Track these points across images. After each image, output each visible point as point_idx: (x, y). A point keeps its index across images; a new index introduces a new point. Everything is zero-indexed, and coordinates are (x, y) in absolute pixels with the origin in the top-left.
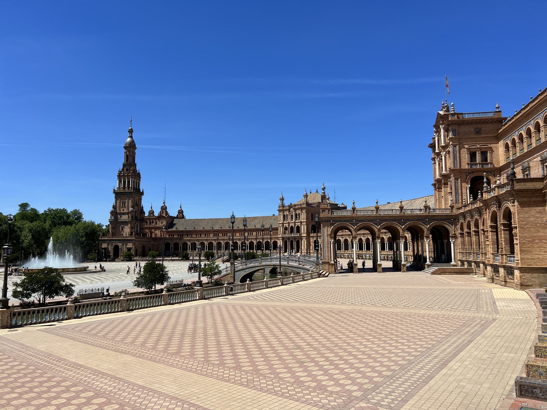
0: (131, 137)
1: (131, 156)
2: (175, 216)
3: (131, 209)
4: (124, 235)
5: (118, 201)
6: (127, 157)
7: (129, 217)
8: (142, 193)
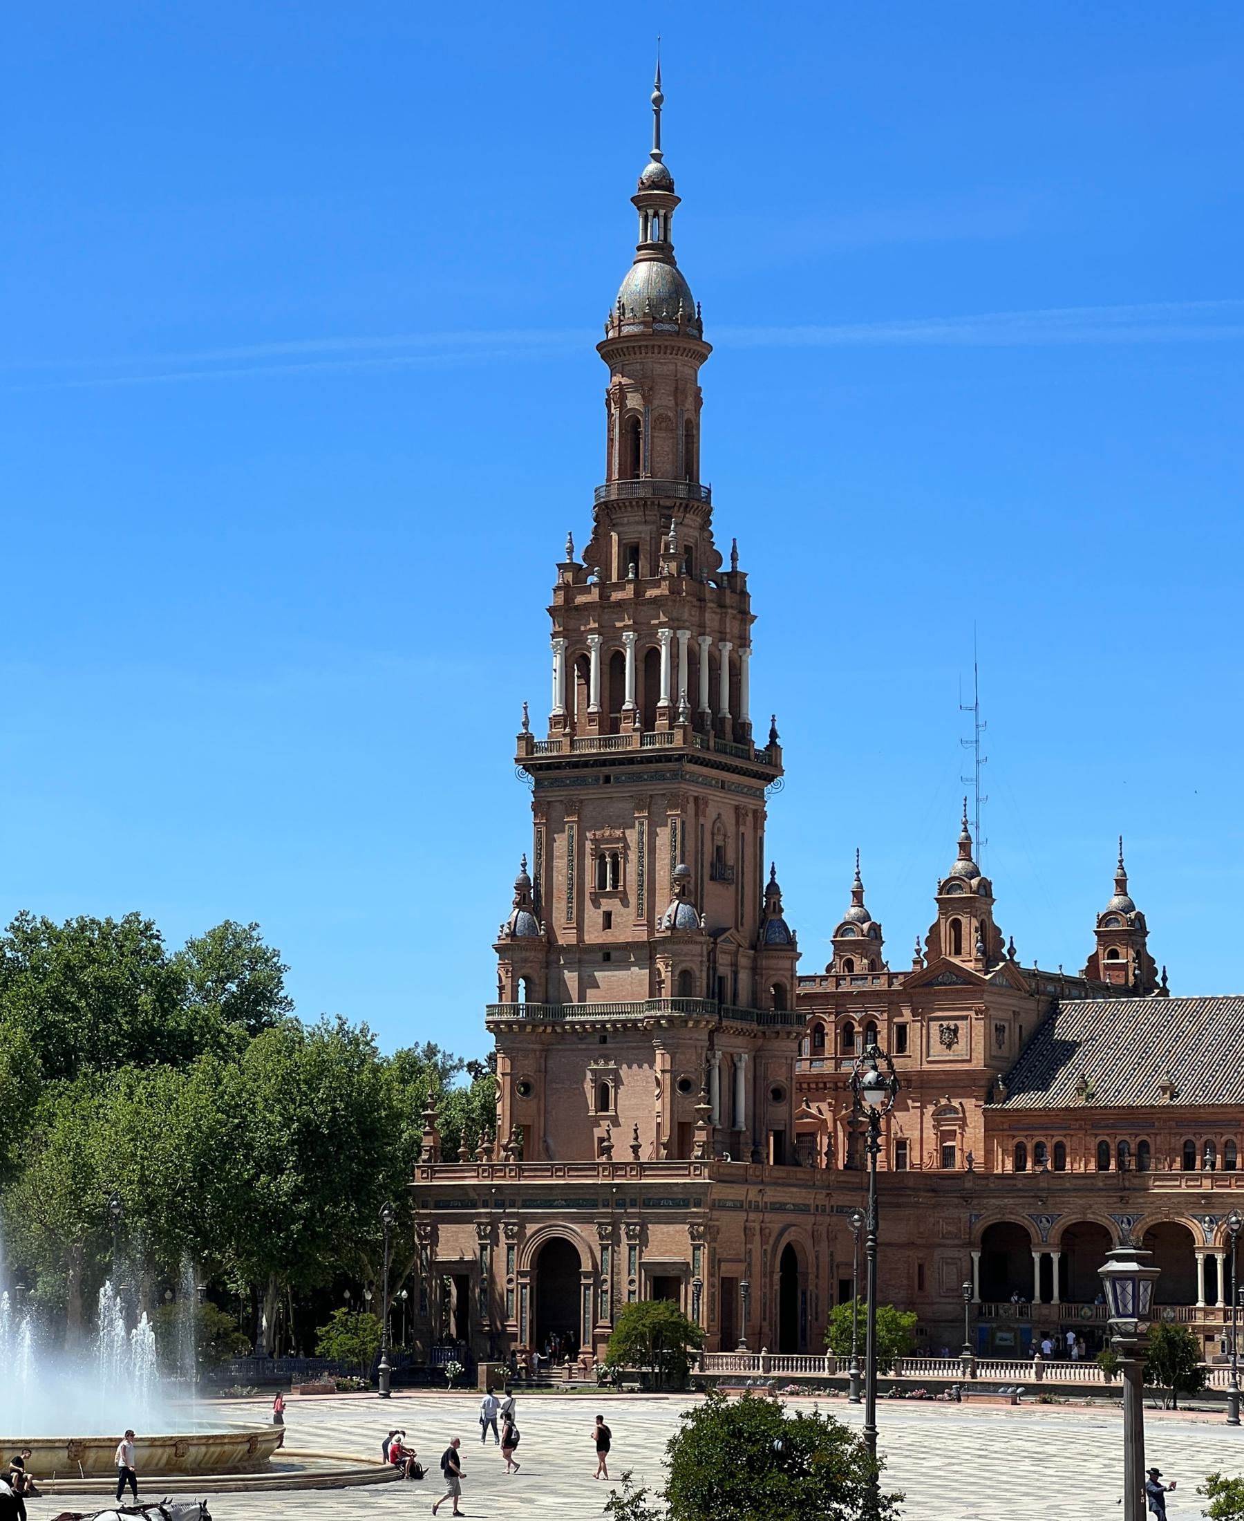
0: (662, 251)
1: (660, 421)
2: (1075, 968)
3: (670, 911)
4: (622, 1154)
5: (561, 843)
6: (631, 430)
7: (655, 985)
8: (768, 766)
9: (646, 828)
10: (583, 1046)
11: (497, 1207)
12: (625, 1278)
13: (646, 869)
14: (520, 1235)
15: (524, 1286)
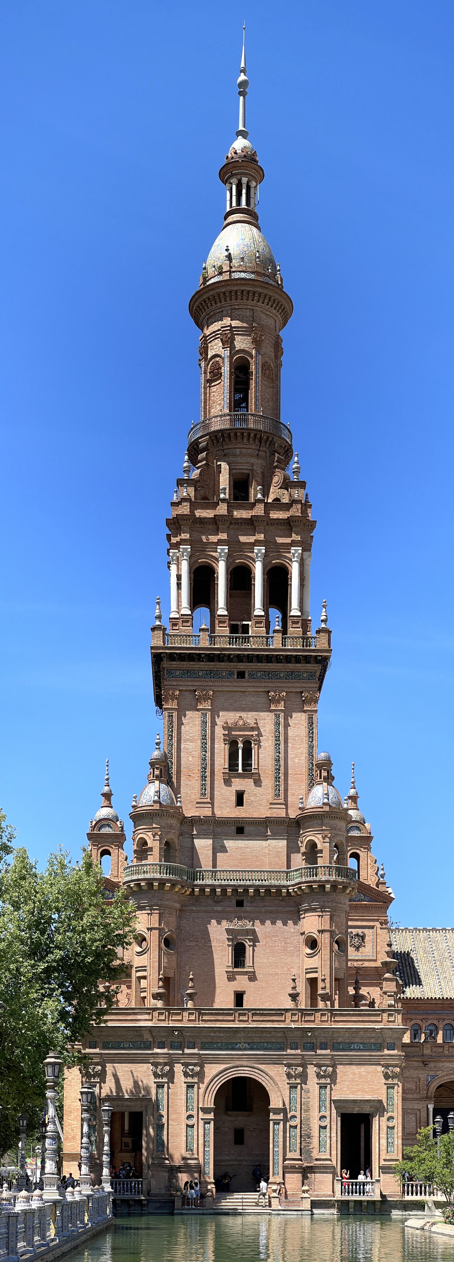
9: (282, 720)
10: (220, 909)
11: (172, 1048)
12: (315, 1114)
13: (282, 755)
14: (200, 1075)
15: (207, 1122)
